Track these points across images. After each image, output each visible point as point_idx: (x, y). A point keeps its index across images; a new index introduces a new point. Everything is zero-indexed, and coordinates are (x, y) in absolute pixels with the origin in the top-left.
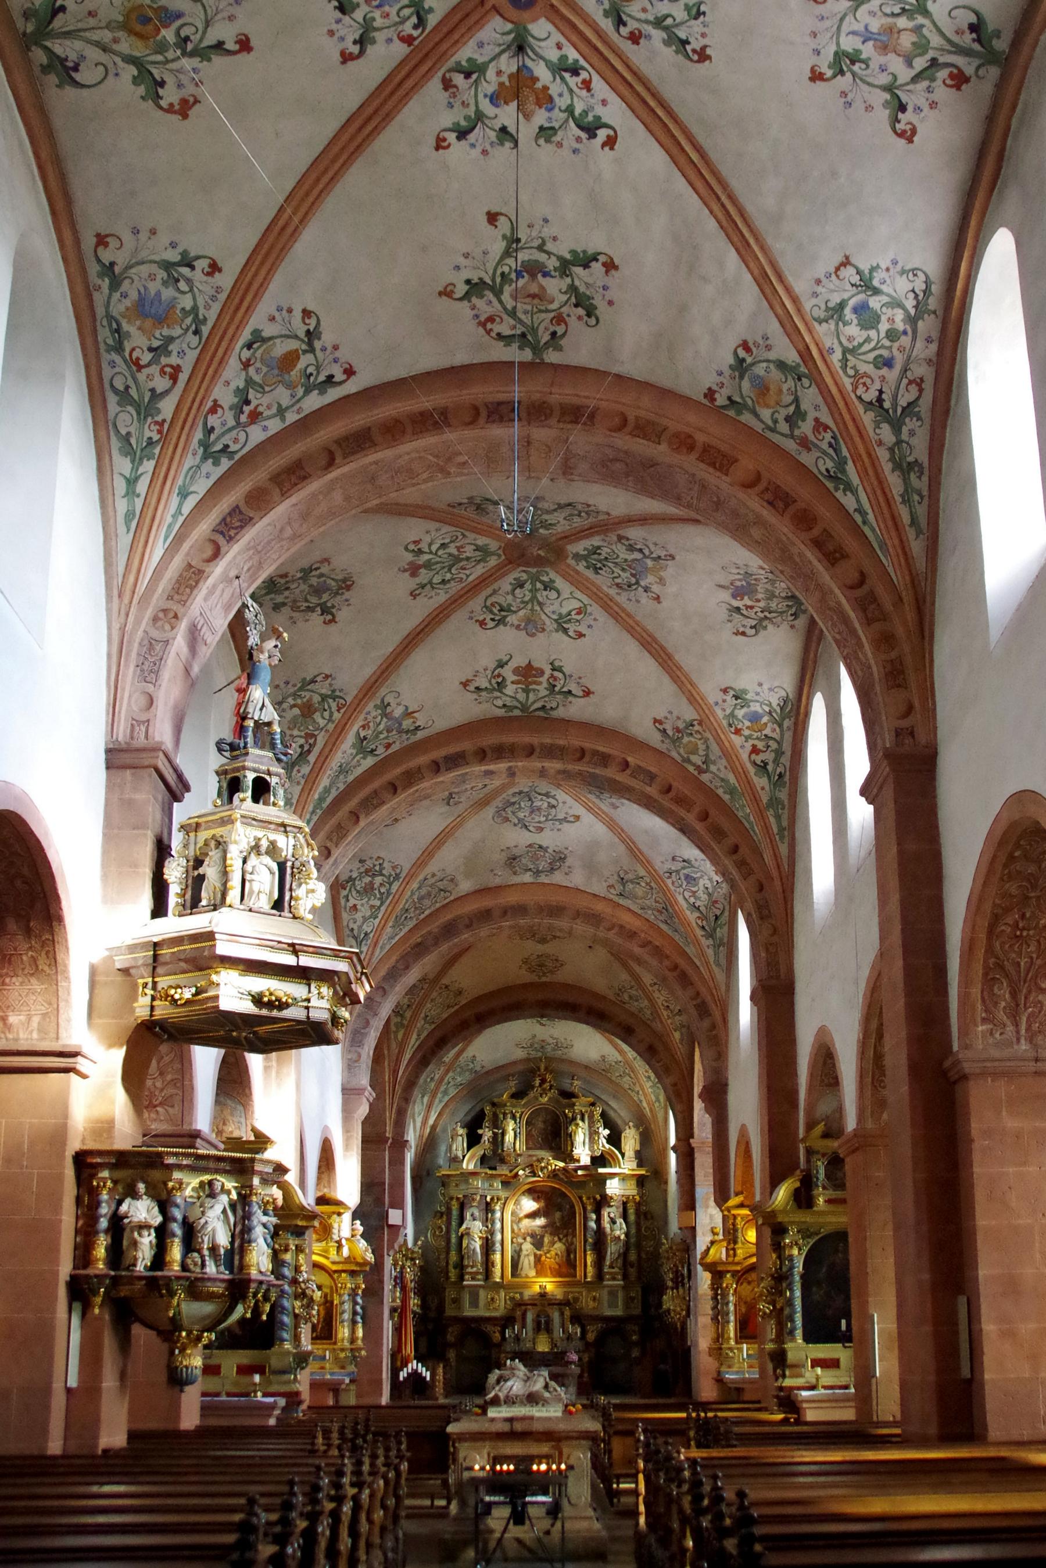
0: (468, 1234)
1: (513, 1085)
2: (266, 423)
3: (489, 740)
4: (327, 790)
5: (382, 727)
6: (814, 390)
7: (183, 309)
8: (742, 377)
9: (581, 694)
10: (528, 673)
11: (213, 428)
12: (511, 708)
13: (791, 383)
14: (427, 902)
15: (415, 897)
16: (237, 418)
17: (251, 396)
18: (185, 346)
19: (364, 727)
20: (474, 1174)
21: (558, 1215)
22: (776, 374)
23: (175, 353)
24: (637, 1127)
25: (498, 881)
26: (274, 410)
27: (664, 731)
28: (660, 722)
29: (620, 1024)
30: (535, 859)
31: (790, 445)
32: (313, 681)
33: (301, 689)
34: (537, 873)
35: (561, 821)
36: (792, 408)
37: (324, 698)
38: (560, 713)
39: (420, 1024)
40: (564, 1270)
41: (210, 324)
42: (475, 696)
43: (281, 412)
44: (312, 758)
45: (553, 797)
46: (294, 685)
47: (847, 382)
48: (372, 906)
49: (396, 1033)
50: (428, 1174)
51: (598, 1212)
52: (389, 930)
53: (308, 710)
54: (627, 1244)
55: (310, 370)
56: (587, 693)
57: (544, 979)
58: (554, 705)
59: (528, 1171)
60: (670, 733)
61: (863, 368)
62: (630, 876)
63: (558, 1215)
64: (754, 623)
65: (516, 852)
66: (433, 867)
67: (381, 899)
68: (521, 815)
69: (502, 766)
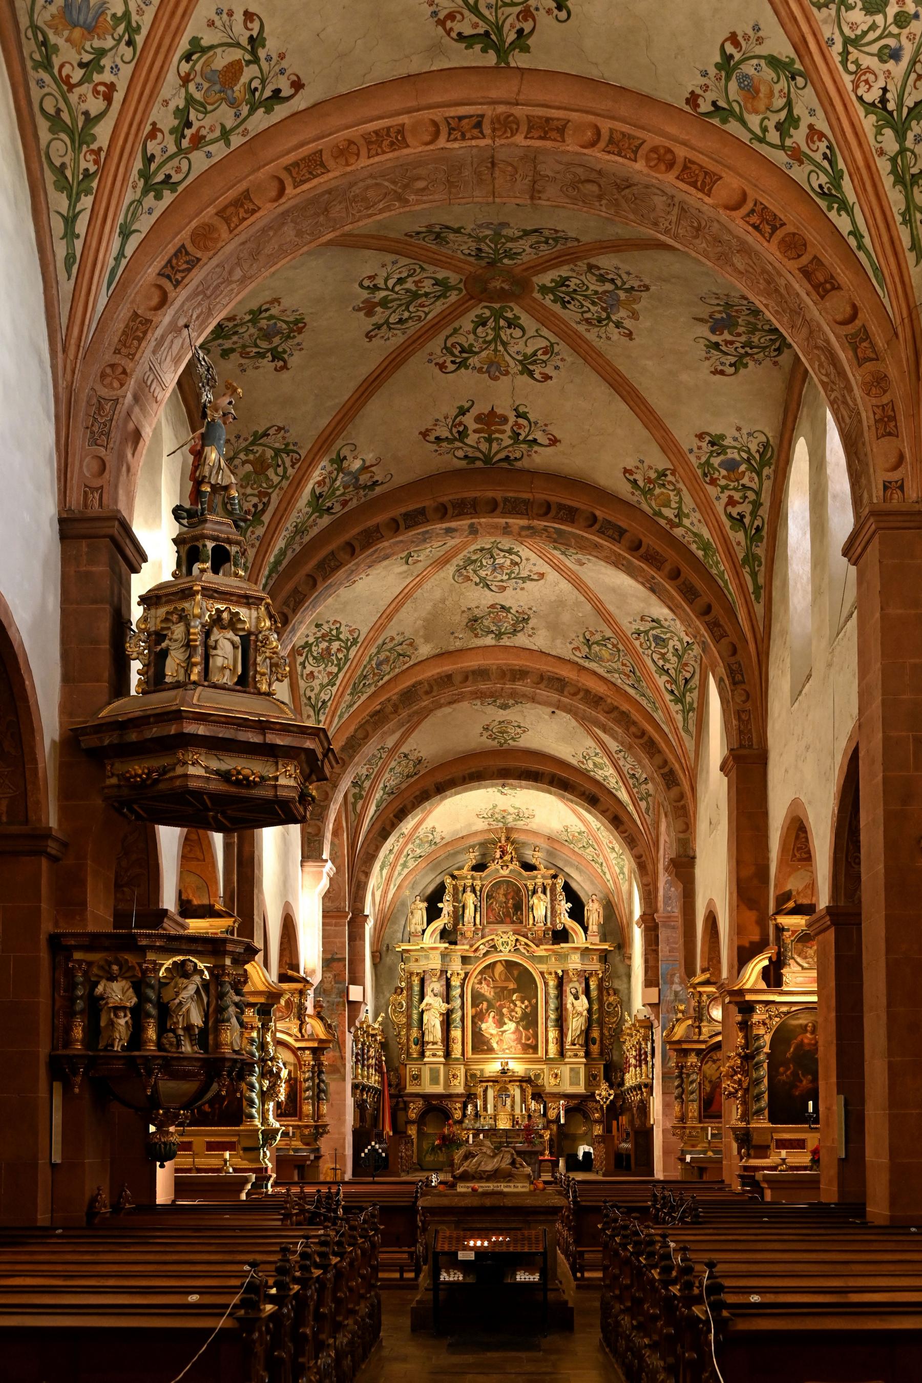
2: (209, 148)
3: (448, 496)
4: (283, 553)
5: (338, 483)
6: (809, 90)
7: (114, 15)
8: (728, 79)
9: (547, 442)
10: (490, 420)
11: (153, 156)
12: (473, 460)
13: (783, 83)
14: (386, 668)
15: (374, 663)
16: (178, 143)
17: (192, 117)
18: (118, 61)
19: (319, 483)
22: (768, 73)
23: (108, 69)
25: (458, 644)
26: (217, 133)
27: (635, 481)
28: (631, 472)
30: (497, 621)
31: (780, 157)
32: (265, 434)
33: (253, 443)
34: (499, 635)
35: (524, 580)
36: (785, 112)
37: (277, 452)
38: (525, 464)
41: (144, 32)
42: (435, 447)
43: (225, 135)
44: (266, 518)
45: (517, 554)
46: (246, 440)
47: (847, 79)
48: (330, 673)
52: (347, 698)
53: (261, 466)
55: (256, 84)
56: (554, 441)
58: (518, 455)
60: (641, 483)
61: (868, 61)
62: (598, 637)
64: (733, 360)
65: (477, 612)
66: (391, 631)
67: (338, 665)
68: (482, 573)
69: (465, 523)
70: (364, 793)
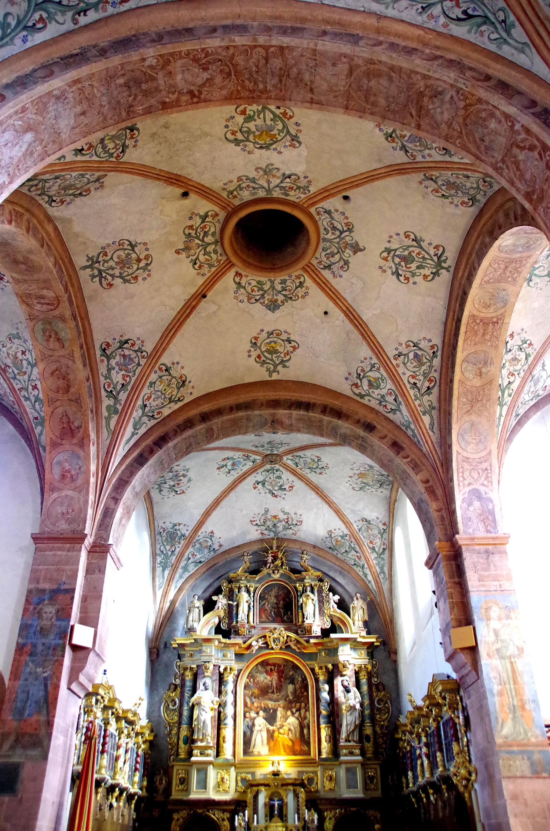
0: (199, 704)
1: (247, 562)
20: (208, 640)
21: (291, 687)
24: (364, 599)
29: (358, 422)
39: (137, 413)
40: (297, 748)
49: (108, 419)
50: (166, 646)
51: (330, 682)
54: (362, 712)
57: (275, 377)
59: (261, 642)
63: (291, 687)
70: (120, 408)
